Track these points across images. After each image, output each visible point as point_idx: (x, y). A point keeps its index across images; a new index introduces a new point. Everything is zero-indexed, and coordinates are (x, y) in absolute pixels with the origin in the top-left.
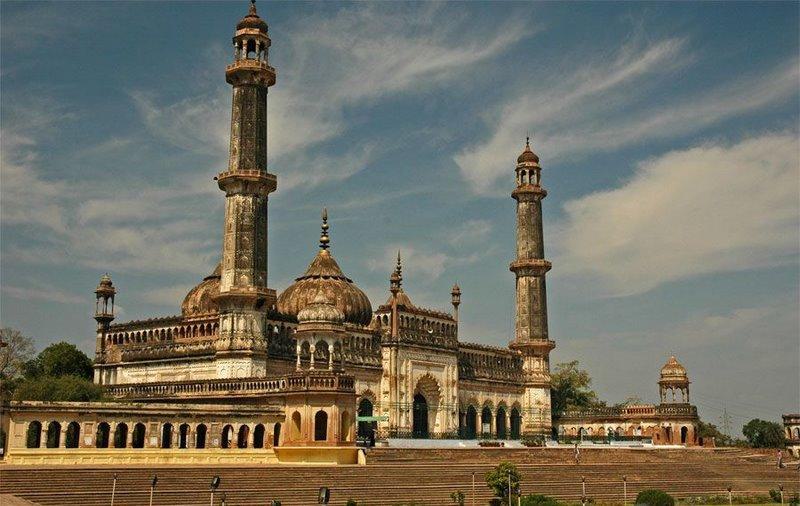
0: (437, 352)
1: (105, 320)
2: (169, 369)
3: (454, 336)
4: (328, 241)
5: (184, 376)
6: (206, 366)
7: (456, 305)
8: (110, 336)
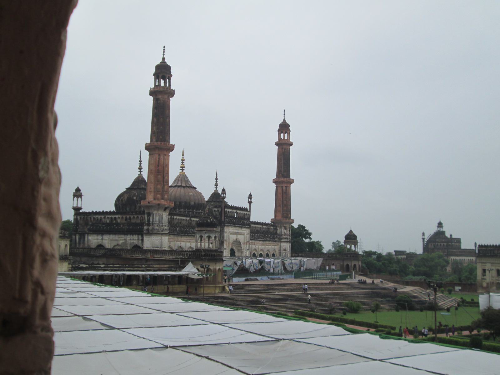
0: (241, 227)
1: (77, 209)
2: (116, 237)
3: (249, 218)
4: (184, 167)
5: (123, 241)
6: (136, 237)
7: (250, 203)
8: (80, 218)
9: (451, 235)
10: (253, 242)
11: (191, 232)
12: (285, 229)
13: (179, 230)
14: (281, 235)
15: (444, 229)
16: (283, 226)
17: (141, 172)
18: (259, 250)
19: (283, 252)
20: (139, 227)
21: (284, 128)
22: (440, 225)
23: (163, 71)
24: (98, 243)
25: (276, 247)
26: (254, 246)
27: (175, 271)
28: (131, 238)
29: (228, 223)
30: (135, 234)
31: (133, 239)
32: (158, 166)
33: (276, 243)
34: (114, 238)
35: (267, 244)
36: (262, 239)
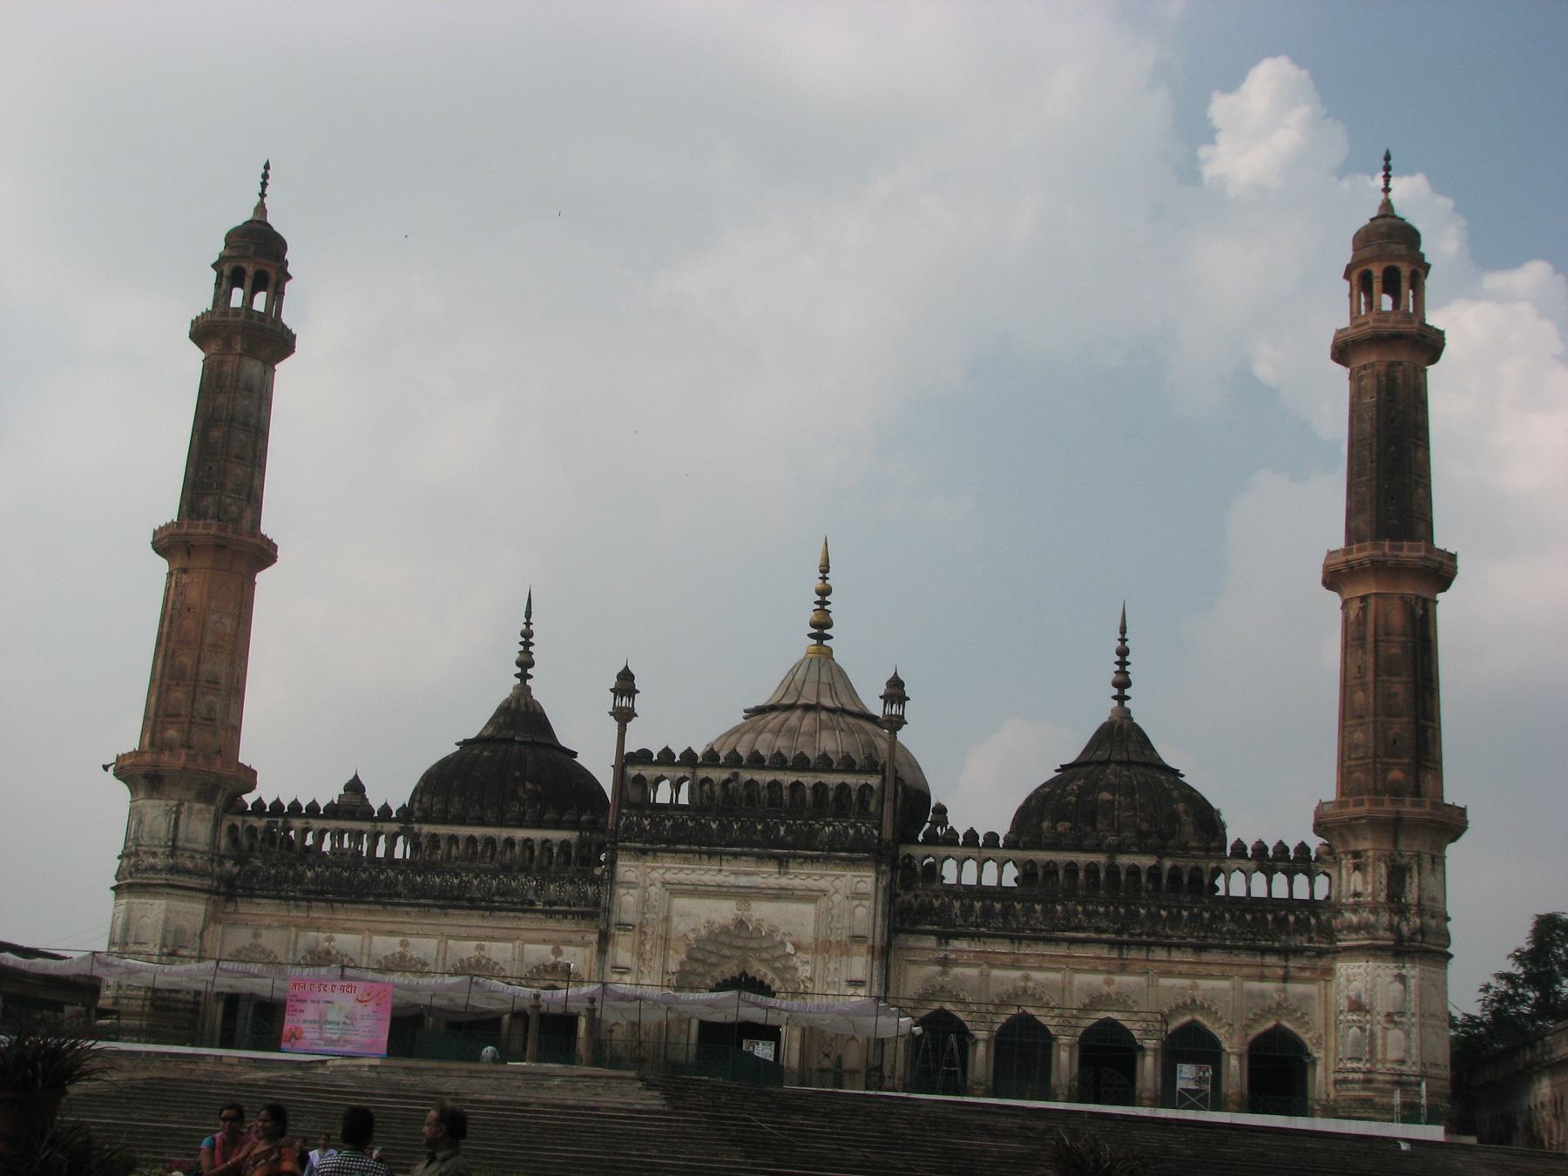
0: (782, 862)
4: (829, 626)
10: (1002, 947)
11: (400, 888)
12: (1357, 867)
13: (312, 881)
16: (1346, 853)
17: (524, 677)
18: (1078, 1000)
23: (255, 256)
25: (1295, 988)
26: (1015, 974)
27: (200, 1045)
29: (641, 834)
33: (1294, 963)
35: (1182, 968)
36: (1098, 930)
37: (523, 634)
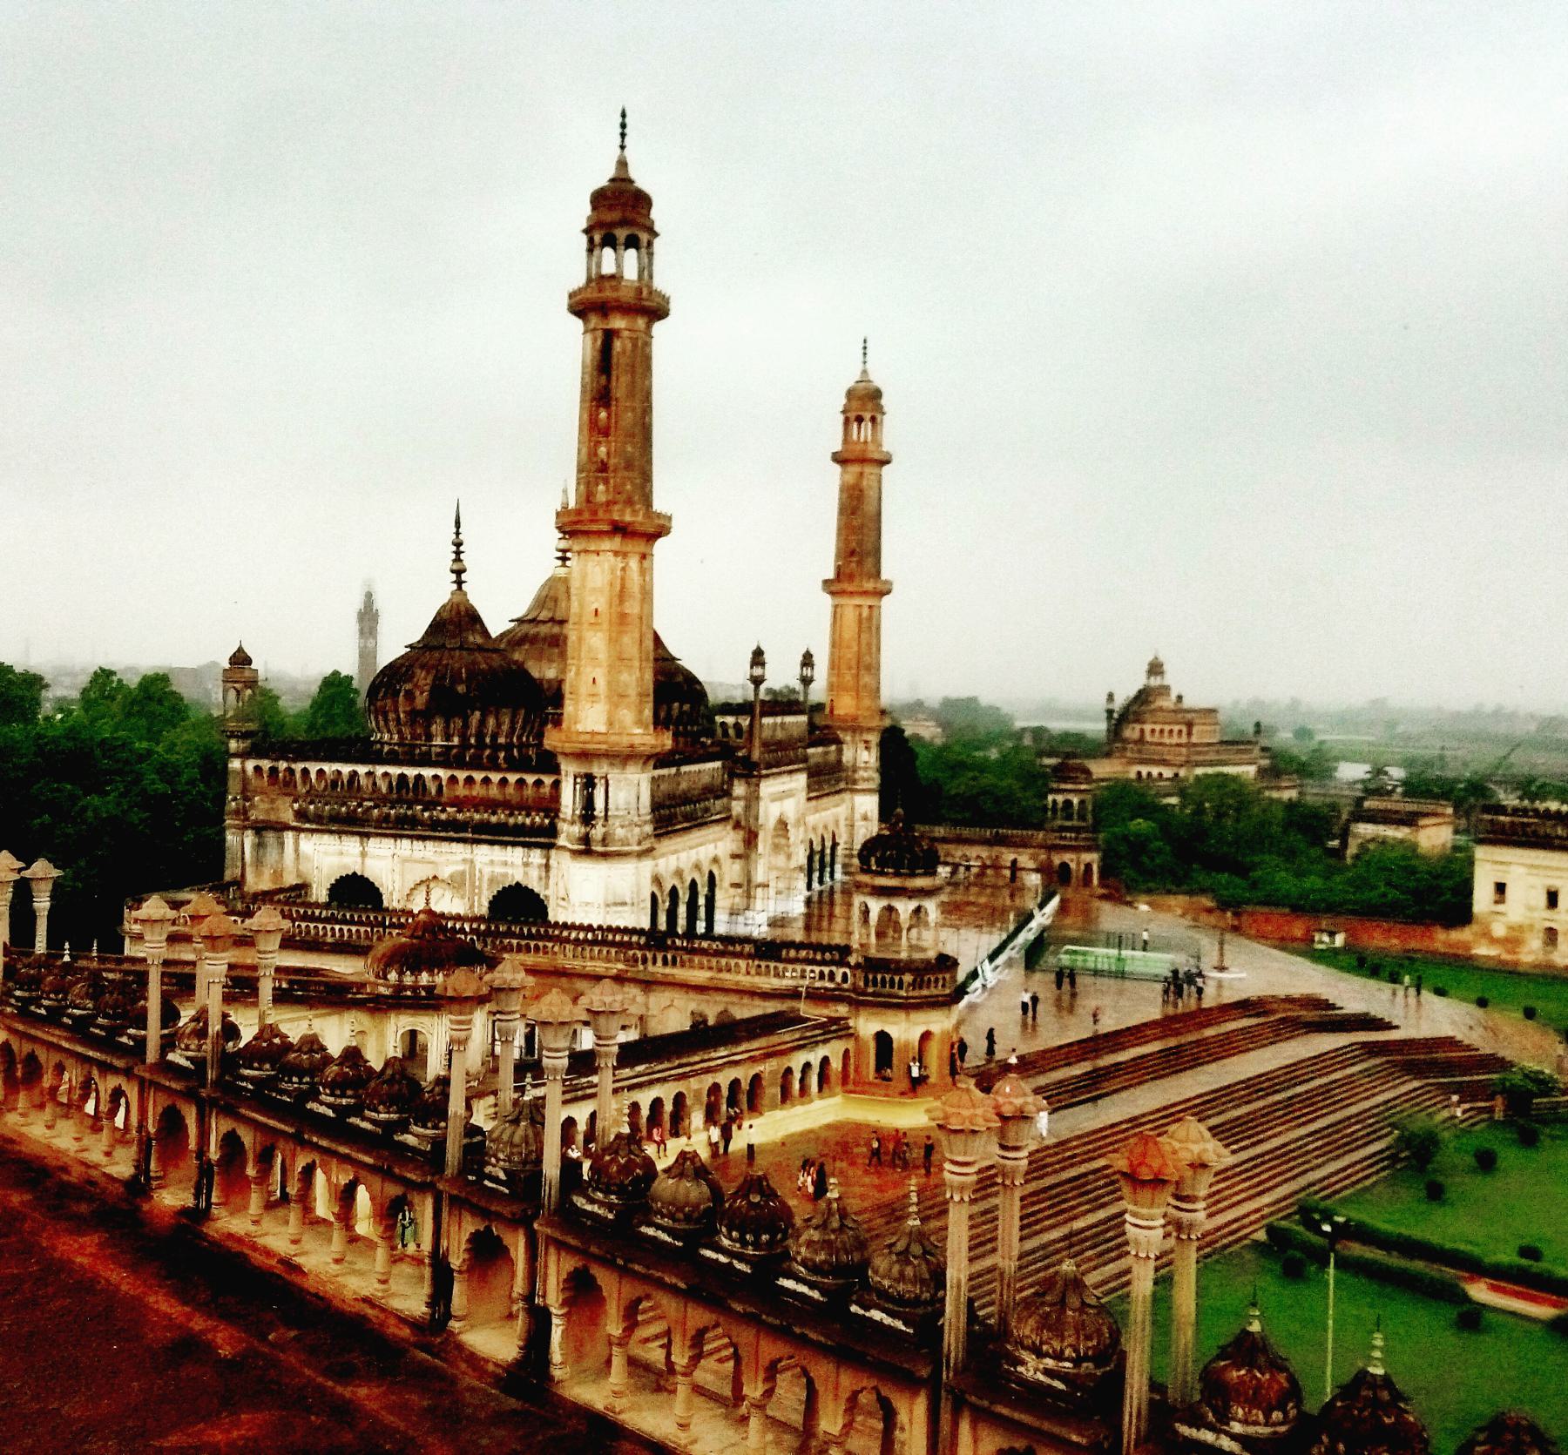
2: (428, 850)
5: (461, 868)
9: (1180, 698)
14: (855, 771)
15: (1168, 679)
17: (459, 583)
19: (859, 823)
20: (528, 821)
21: (864, 404)
22: (1155, 668)
24: (345, 867)
25: (839, 809)
28: (496, 859)
30: (514, 844)
31: (506, 863)
32: (622, 595)
34: (418, 855)
37: (454, 544)
